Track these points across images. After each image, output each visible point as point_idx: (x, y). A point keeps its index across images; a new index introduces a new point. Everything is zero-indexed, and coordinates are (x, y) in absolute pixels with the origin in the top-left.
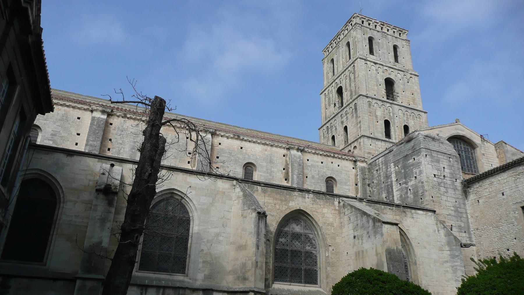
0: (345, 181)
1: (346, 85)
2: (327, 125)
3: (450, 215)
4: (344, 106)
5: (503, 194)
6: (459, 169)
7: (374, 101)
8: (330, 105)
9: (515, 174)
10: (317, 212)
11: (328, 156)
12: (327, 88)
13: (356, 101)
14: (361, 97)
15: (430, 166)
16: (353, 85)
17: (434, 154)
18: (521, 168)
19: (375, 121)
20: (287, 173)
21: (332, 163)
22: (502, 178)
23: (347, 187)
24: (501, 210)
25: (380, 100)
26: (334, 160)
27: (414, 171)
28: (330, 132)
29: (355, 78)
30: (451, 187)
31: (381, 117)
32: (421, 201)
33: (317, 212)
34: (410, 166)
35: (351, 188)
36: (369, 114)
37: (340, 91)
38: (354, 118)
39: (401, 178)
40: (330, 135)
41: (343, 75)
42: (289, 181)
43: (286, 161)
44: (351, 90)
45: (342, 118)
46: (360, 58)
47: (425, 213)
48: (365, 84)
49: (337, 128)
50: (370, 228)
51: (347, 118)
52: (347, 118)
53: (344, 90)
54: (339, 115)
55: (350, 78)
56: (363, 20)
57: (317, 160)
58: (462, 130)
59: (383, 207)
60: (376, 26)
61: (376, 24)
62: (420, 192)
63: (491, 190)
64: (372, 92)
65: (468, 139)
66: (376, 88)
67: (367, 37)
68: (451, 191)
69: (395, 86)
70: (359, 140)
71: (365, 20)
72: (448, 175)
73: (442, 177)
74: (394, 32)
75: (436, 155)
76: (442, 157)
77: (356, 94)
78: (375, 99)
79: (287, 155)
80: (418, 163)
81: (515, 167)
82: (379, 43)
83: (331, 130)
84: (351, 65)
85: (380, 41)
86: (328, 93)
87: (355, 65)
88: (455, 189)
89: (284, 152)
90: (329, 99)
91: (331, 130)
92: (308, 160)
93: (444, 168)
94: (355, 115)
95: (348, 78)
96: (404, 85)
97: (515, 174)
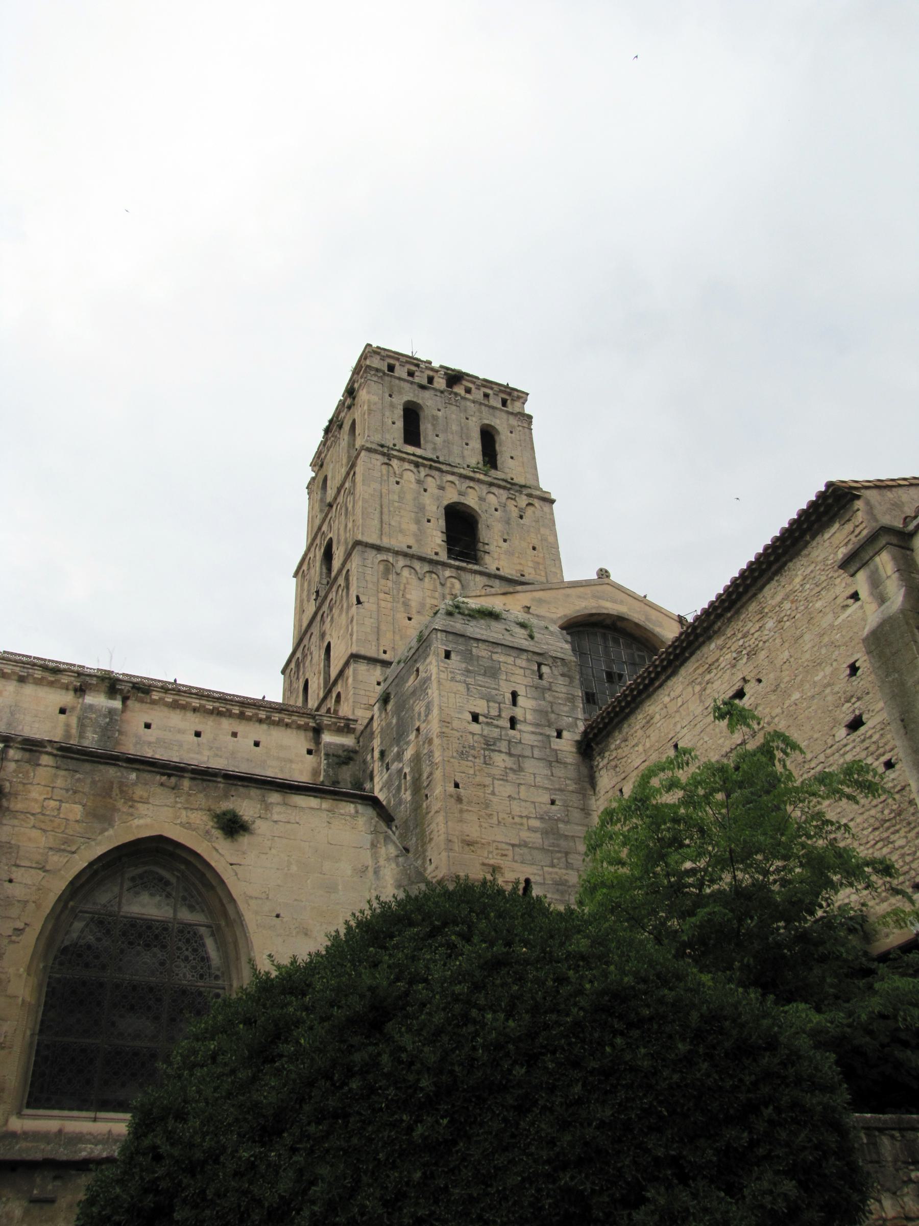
1: (339, 529)
3: (524, 844)
6: (571, 699)
7: (401, 562)
8: (308, 601)
9: (700, 671)
11: (220, 714)
14: (359, 548)
15: (462, 688)
16: (350, 525)
17: (481, 651)
18: (713, 646)
19: (401, 616)
21: (235, 735)
22: (673, 695)
26: (241, 728)
27: (417, 709)
28: (301, 673)
30: (537, 753)
31: (423, 605)
36: (382, 595)
39: (391, 746)
40: (301, 680)
43: (68, 726)
46: (369, 450)
47: (326, 804)
48: (377, 515)
55: (347, 509)
56: (392, 362)
58: (615, 602)
59: (133, 776)
63: (648, 745)
64: (400, 537)
65: (637, 625)
66: (413, 527)
67: (399, 402)
68: (534, 769)
69: (480, 526)
71: (397, 364)
72: (529, 717)
74: (486, 396)
75: (484, 653)
76: (510, 660)
78: (405, 555)
81: (698, 648)
82: (435, 418)
85: (440, 414)
88: (553, 760)
89: (67, 698)
91: (304, 665)
93: (514, 695)
96: (508, 522)
97: (700, 671)
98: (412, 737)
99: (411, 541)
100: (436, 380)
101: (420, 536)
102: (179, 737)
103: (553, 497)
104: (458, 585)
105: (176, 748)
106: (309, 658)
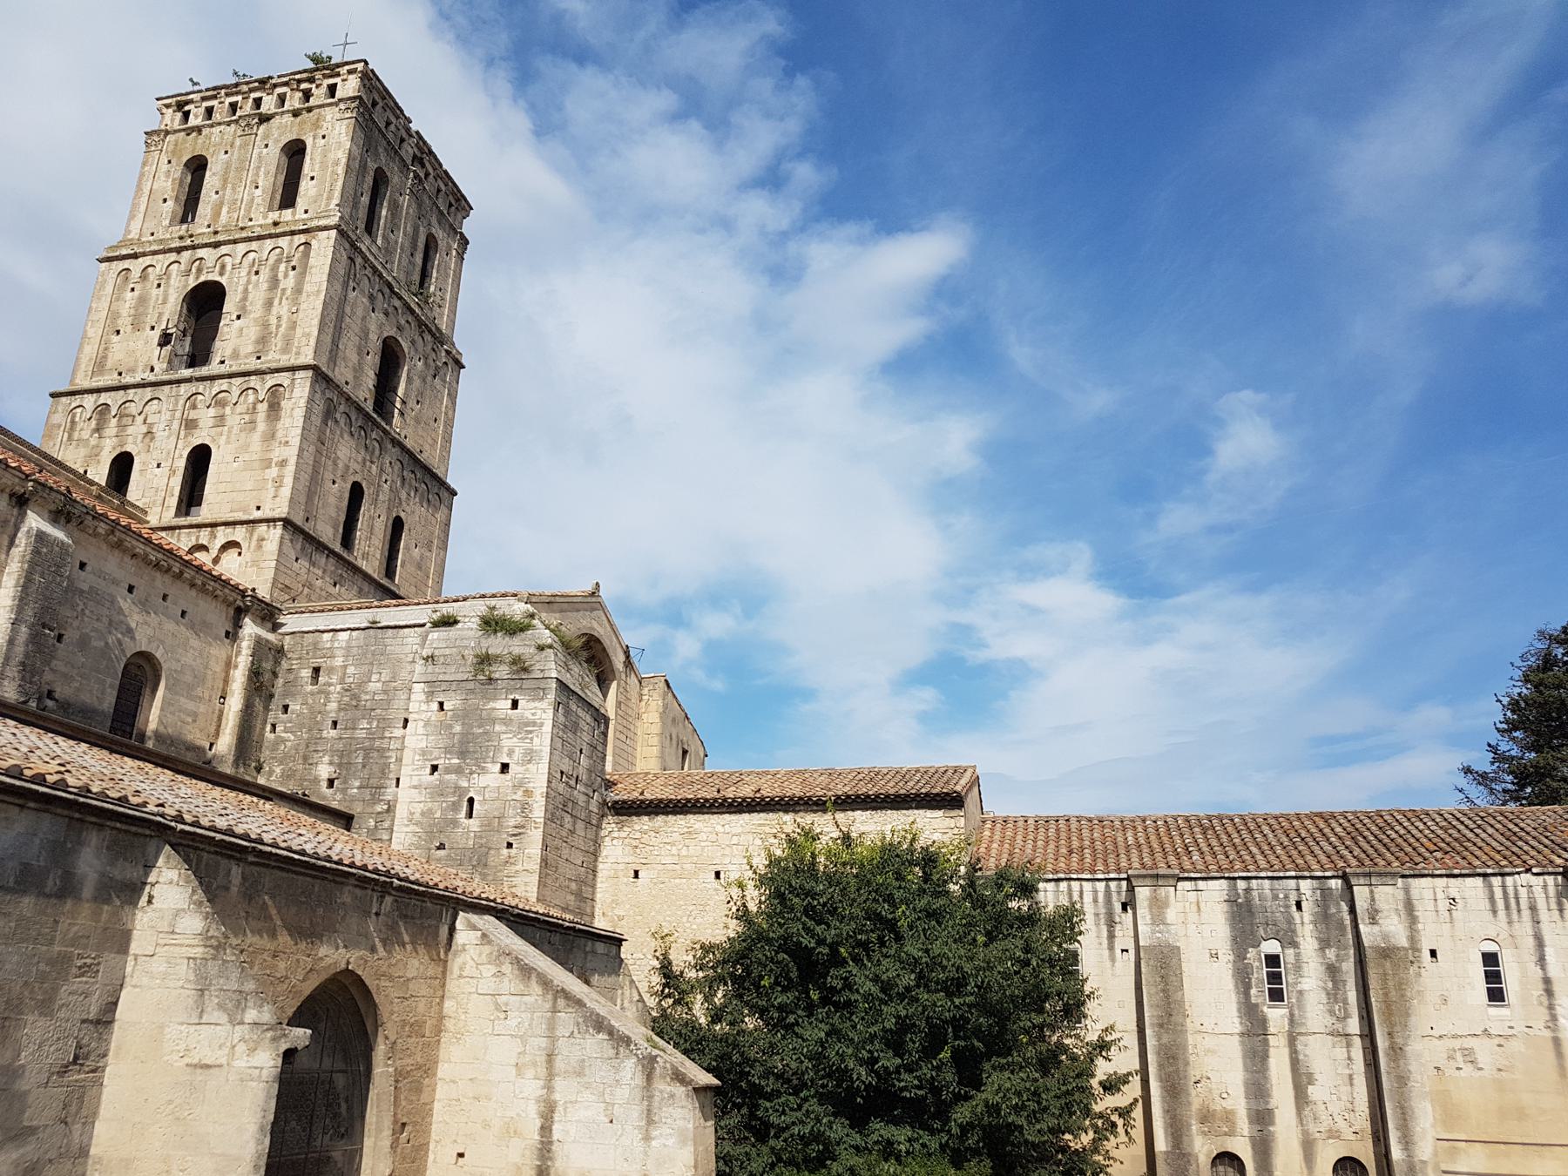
0: (188, 678)
1: (246, 290)
2: (105, 398)
4: (213, 368)
5: (718, 875)
8: (136, 326)
10: (391, 978)
12: (144, 254)
13: (284, 378)
16: (282, 309)
21: (165, 597)
23: (190, 706)
24: (699, 920)
25: (359, 409)
29: (298, 290)
31: (347, 467)
32: (505, 851)
33: (391, 978)
34: (493, 721)
35: (202, 708)
37: (206, 303)
38: (256, 437)
41: (242, 248)
44: (266, 325)
45: (194, 407)
50: (623, 1093)
51: (220, 420)
52: (220, 420)
53: (229, 306)
54: (185, 390)
55: (274, 282)
57: (118, 574)
60: (402, 140)
62: (512, 822)
63: (684, 852)
70: (263, 528)
73: (572, 783)
80: (527, 725)
83: (122, 427)
84: (293, 233)
87: (314, 242)
90: (142, 300)
91: (122, 427)
92: (82, 566)
95: (265, 274)
99: (350, 378)
100: (405, 145)
101: (358, 370)
102: (112, 589)
104: (377, 452)
105: (108, 604)
106: (137, 429)
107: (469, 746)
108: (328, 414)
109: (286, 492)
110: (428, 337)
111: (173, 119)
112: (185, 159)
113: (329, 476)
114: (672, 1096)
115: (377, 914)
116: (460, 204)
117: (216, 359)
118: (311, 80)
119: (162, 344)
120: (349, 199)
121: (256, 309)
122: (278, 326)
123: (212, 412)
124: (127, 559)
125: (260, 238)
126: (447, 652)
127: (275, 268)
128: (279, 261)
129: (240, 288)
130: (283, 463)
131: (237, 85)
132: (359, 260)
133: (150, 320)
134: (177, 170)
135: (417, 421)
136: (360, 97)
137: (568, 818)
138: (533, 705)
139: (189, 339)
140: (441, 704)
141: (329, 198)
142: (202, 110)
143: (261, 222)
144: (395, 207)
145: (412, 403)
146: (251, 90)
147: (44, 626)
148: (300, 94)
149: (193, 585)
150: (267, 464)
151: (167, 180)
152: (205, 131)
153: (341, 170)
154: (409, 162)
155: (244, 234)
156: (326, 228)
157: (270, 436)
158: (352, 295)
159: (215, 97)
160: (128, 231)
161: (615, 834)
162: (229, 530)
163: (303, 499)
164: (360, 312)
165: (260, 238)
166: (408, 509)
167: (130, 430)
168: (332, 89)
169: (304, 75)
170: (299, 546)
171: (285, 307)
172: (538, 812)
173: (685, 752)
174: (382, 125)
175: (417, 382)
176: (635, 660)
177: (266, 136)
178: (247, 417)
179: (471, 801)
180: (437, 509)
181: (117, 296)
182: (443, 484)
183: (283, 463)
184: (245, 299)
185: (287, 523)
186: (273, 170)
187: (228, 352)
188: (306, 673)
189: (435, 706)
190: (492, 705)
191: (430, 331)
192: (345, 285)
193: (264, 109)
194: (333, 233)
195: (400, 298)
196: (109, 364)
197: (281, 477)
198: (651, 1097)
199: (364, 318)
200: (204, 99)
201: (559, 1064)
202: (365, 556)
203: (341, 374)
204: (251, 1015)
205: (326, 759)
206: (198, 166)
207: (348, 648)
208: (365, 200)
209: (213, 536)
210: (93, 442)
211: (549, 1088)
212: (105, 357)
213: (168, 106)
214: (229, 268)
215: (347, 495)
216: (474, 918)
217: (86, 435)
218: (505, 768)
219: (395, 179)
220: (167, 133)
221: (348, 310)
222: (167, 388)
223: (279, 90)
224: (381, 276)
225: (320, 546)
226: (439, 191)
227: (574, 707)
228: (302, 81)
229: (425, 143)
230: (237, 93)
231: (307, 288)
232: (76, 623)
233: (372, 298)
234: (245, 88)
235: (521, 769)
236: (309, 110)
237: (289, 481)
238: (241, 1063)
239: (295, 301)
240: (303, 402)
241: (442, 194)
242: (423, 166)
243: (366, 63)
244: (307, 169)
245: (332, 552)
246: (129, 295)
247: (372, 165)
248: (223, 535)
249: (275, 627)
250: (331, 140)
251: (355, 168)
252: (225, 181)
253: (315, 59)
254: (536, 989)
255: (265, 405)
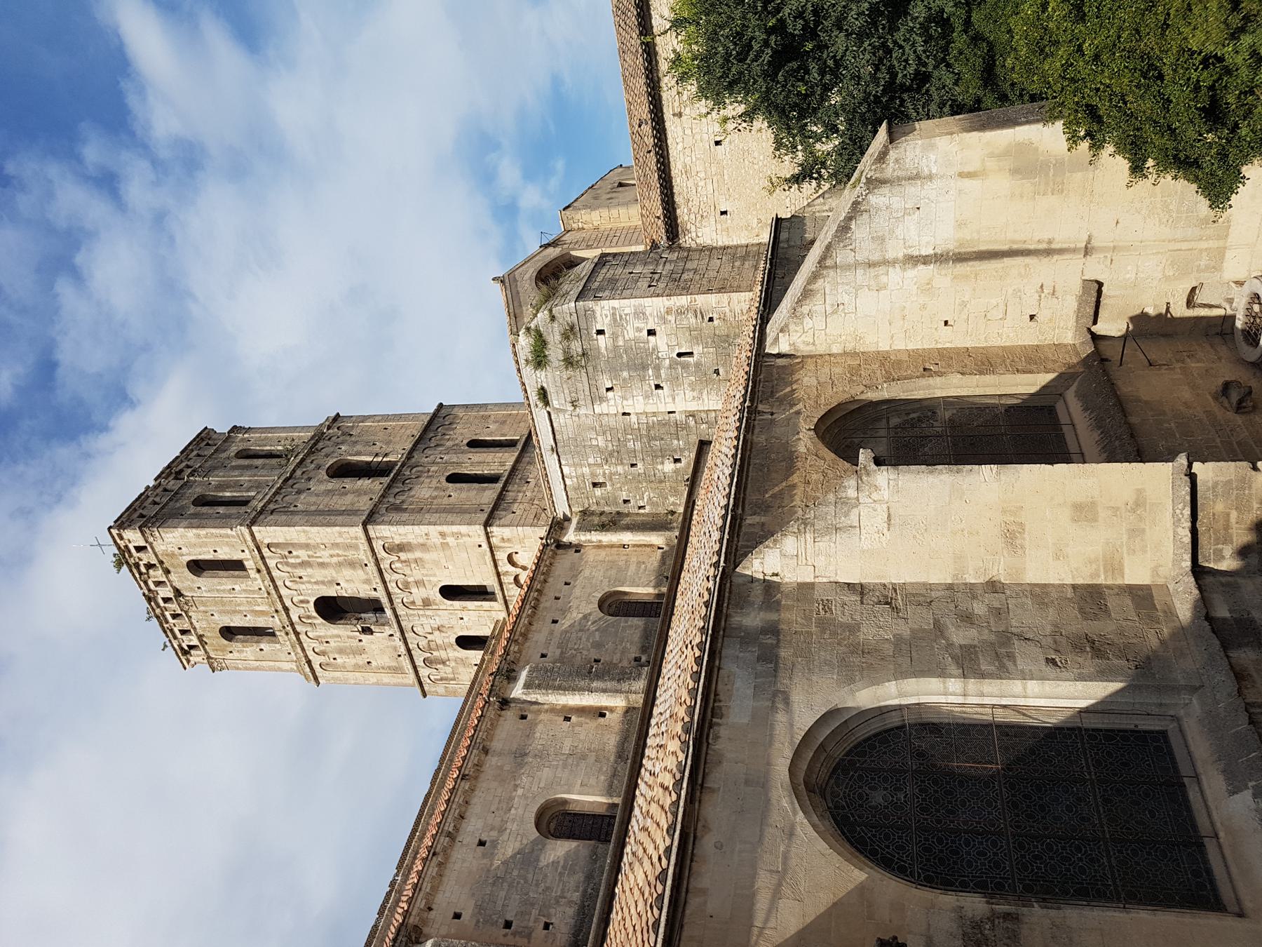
0: (613, 572)
2: (419, 662)
4: (381, 595)
5: (717, 143)
8: (362, 651)
10: (819, 396)
12: (306, 656)
13: (378, 545)
16: (324, 555)
20: (582, 711)
21: (557, 598)
23: (633, 568)
24: (756, 154)
25: (389, 487)
28: (442, 654)
29: (307, 546)
32: (716, 322)
33: (819, 396)
34: (616, 347)
35: (634, 559)
37: (331, 609)
38: (426, 556)
41: (283, 591)
42: (606, 708)
44: (340, 564)
45: (413, 603)
49: (438, 622)
50: (896, 202)
54: (401, 611)
55: (304, 564)
60: (165, 490)
61: (161, 489)
62: (693, 320)
63: (702, 175)
70: (494, 541)
73: (656, 276)
77: (356, 547)
79: (521, 709)
80: (615, 320)
83: (438, 648)
84: (263, 558)
86: (323, 653)
87: (266, 542)
92: (543, 656)
94: (418, 554)
98: (651, 338)
99: (366, 498)
100: (169, 487)
101: (358, 493)
102: (557, 634)
103: (333, 415)
106: (437, 637)
107: (638, 363)
108: (398, 508)
109: (464, 529)
110: (320, 445)
111: (197, 656)
112: (226, 642)
113: (446, 501)
114: (897, 161)
115: (772, 414)
116: (204, 438)
117: (373, 594)
118: (137, 566)
119: (371, 632)
120: (224, 521)
121: (329, 573)
122: (338, 555)
123: (414, 590)
124: (533, 628)
125: (273, 580)
126: (566, 391)
127: (294, 566)
128: (287, 564)
129: (315, 587)
130: (443, 535)
131: (157, 617)
132: (272, 506)
133: (355, 643)
134: (235, 646)
135: (388, 443)
136: (140, 528)
137: (685, 276)
138: (599, 318)
139: (363, 615)
140: (608, 390)
141: (228, 536)
142: (184, 637)
143: (260, 581)
144: (221, 487)
145: (376, 449)
146: (159, 606)
147: (590, 672)
148: (151, 571)
149: (545, 581)
150: (445, 546)
151: (245, 651)
152: (200, 632)
153: (203, 532)
154: (181, 482)
155: (273, 592)
156: (252, 535)
157: (423, 546)
158: (300, 507)
159: (172, 631)
160: (292, 670)
161: (694, 235)
162: (500, 563)
163: (468, 516)
164: (313, 499)
165: (273, 580)
166: (460, 438)
167: (439, 642)
168: (139, 549)
169: (135, 571)
170: (503, 513)
171: (322, 552)
172: (683, 301)
173: (621, 185)
174: (158, 507)
175: (359, 447)
176: (551, 238)
177: (191, 589)
178: (413, 565)
179: (679, 355)
180: (456, 417)
181: (343, 668)
182: (435, 415)
183: (443, 535)
184: (323, 583)
185: (487, 524)
186: (216, 580)
187: (367, 587)
188: (598, 492)
189: (610, 394)
190: (603, 350)
191: (315, 444)
192: (293, 513)
193: (171, 595)
194: (254, 529)
195: (294, 471)
196: (394, 664)
197: (453, 534)
198: (899, 179)
199: (317, 495)
200: (175, 638)
201: (876, 257)
202: (502, 464)
203: (365, 504)
204: (851, 493)
205: (660, 467)
206: (229, 633)
207: (575, 465)
208: (221, 510)
209: (506, 573)
210: (453, 664)
211: (893, 263)
212: (389, 668)
213: (188, 661)
214: (301, 598)
215: (458, 485)
216: (769, 340)
217: (449, 670)
218: (651, 333)
219: (198, 490)
220: (209, 658)
221: (313, 508)
222: (403, 624)
223: (152, 586)
224: (280, 488)
225: (500, 497)
226: (198, 455)
227: (597, 284)
228: (140, 573)
229: (162, 473)
230: (164, 616)
231: (303, 540)
232: (585, 652)
233: (299, 492)
234: (158, 611)
235: (651, 320)
236: (161, 563)
237: (455, 528)
238: (885, 494)
239: (316, 547)
240: (393, 528)
241: (201, 453)
242: (181, 471)
243: (110, 528)
244: (209, 556)
245: (504, 488)
246: (339, 660)
247: (192, 509)
248: (504, 567)
249: (567, 519)
250: (181, 543)
251: (198, 521)
252: (235, 612)
253: (119, 565)
254: (820, 283)
255: (401, 554)
